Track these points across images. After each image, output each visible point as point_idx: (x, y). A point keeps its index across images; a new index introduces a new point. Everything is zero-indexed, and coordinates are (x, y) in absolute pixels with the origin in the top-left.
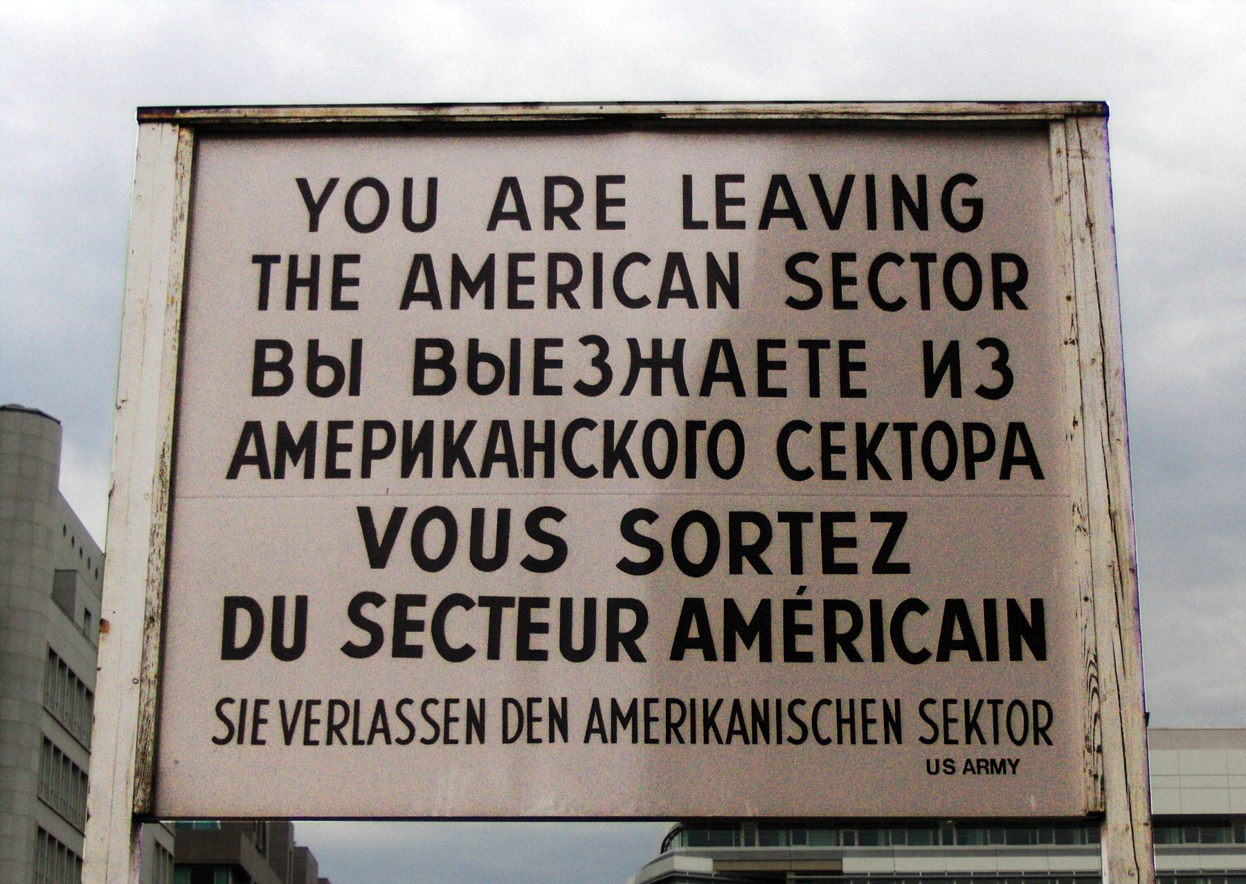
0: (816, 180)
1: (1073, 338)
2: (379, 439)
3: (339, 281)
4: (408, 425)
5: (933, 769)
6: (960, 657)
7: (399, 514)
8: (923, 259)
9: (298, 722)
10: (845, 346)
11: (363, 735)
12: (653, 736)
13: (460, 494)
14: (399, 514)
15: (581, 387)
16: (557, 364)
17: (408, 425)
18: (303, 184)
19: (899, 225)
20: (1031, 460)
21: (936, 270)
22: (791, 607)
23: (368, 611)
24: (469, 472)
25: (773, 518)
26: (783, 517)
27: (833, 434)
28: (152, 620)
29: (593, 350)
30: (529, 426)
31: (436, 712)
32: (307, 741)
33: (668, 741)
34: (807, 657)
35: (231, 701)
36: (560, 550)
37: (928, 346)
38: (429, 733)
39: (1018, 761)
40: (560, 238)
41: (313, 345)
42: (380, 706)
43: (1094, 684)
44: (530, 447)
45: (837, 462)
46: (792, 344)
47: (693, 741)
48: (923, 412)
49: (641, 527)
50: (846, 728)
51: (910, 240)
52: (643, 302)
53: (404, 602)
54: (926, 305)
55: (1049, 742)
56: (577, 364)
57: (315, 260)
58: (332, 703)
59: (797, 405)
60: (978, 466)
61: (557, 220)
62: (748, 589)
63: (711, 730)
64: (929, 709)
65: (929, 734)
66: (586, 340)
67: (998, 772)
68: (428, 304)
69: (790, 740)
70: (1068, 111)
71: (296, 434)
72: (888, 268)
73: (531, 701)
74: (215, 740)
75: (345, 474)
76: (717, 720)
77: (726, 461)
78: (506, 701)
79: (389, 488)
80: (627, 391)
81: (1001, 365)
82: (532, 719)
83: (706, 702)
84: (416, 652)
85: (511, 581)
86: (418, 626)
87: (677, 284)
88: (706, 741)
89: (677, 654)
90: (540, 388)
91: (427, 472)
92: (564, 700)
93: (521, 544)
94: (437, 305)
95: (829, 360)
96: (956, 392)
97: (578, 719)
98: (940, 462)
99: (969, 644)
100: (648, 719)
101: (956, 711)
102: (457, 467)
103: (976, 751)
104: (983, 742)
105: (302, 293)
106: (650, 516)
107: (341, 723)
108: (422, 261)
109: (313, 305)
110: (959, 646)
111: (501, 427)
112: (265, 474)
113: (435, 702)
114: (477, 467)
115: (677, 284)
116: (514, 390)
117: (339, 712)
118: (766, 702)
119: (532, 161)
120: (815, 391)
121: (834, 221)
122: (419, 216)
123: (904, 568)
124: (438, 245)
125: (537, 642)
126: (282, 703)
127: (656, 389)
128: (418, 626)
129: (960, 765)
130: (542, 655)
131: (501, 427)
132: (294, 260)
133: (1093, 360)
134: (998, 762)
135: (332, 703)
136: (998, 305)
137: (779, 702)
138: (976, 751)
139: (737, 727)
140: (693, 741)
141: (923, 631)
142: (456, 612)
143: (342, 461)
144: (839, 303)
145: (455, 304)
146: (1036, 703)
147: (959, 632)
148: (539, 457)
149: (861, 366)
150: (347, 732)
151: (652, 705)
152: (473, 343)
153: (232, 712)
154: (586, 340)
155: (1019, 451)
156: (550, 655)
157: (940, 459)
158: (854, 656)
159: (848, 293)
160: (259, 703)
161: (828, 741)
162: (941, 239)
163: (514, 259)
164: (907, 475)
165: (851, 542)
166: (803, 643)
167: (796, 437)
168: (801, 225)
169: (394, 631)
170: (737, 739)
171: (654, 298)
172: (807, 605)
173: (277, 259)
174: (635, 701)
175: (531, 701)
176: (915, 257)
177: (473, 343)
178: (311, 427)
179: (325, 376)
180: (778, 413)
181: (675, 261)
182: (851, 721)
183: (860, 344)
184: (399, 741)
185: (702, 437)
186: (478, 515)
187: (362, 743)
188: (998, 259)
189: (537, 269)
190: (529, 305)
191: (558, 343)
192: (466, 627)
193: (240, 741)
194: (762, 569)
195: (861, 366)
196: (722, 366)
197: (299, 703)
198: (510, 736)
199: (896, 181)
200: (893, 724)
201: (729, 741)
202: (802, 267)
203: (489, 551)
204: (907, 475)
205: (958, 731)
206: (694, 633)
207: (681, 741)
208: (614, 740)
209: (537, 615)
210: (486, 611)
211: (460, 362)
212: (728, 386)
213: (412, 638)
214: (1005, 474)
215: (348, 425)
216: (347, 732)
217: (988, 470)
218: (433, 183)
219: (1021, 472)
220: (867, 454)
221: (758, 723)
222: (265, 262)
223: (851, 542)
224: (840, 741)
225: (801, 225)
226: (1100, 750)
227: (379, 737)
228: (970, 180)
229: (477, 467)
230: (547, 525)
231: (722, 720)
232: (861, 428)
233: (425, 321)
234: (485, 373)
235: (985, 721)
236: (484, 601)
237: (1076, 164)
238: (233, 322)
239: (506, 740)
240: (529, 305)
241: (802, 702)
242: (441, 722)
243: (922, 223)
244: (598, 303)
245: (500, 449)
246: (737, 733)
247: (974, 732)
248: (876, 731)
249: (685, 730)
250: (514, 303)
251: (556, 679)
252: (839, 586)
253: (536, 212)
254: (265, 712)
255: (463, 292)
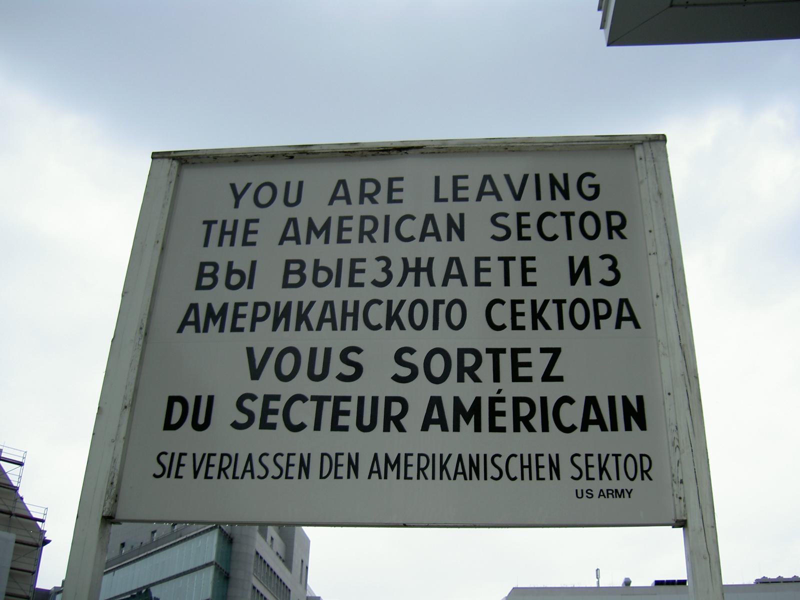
0: (508, 177)
1: (654, 251)
2: (262, 311)
3: (247, 232)
4: (278, 304)
5: (580, 495)
6: (594, 429)
7: (269, 351)
8: (568, 215)
9: (203, 466)
10: (524, 260)
11: (239, 473)
12: (408, 476)
13: (303, 340)
14: (269, 351)
15: (375, 283)
16: (363, 271)
17: (278, 304)
18: (233, 186)
19: (553, 197)
20: (633, 318)
21: (575, 221)
22: (493, 401)
23: (247, 404)
24: (310, 328)
25: (483, 352)
26: (488, 351)
27: (517, 305)
28: (126, 407)
29: (383, 264)
30: (345, 304)
31: (282, 461)
32: (206, 477)
33: (418, 478)
34: (503, 430)
35: (166, 453)
36: (359, 369)
37: (571, 259)
38: (277, 475)
39: (631, 490)
40: (368, 208)
41: (230, 264)
42: (250, 456)
43: (676, 443)
44: (345, 314)
45: (520, 321)
46: (494, 259)
47: (433, 478)
48: (570, 293)
49: (406, 357)
50: (526, 470)
51: (560, 205)
52: (412, 239)
53: (268, 398)
54: (569, 237)
55: (650, 479)
56: (374, 271)
57: (236, 222)
58: (223, 455)
59: (497, 290)
60: (602, 322)
61: (366, 200)
62: (468, 392)
63: (444, 472)
64: (576, 459)
65: (577, 474)
66: (379, 259)
67: (620, 496)
68: (294, 242)
69: (492, 478)
70: (644, 139)
71: (217, 310)
72: (548, 219)
73: (337, 455)
74: (155, 476)
75: (241, 330)
76: (448, 466)
77: (456, 321)
78: (323, 455)
79: (265, 337)
80: (400, 284)
81: (613, 268)
82: (337, 465)
83: (441, 455)
84: (273, 426)
85: (331, 387)
86: (275, 412)
87: (430, 229)
88: (441, 478)
89: (425, 428)
90: (352, 284)
91: (287, 328)
92: (357, 454)
93: (337, 366)
94: (298, 243)
95: (515, 268)
96: (588, 282)
97: (364, 466)
98: (580, 320)
99: (600, 422)
100: (406, 465)
101: (593, 461)
102: (303, 326)
103: (606, 484)
104: (610, 479)
105: (227, 238)
106: (411, 351)
107: (225, 466)
108: (293, 221)
109: (232, 244)
110: (594, 422)
111: (328, 304)
112: (198, 330)
113: (282, 455)
114: (314, 324)
115: (430, 229)
116: (338, 285)
117: (226, 459)
118: (478, 456)
119: (353, 173)
120: (507, 283)
121: (518, 197)
122: (292, 198)
123: (560, 379)
124: (301, 214)
125: (342, 421)
126: (194, 455)
127: (417, 283)
128: (275, 412)
129: (596, 493)
130: (345, 429)
131: (328, 304)
132: (224, 222)
133: (666, 263)
134: (620, 492)
135: (223, 455)
136: (610, 237)
137: (485, 456)
138: (606, 484)
139: (460, 470)
140: (433, 478)
141: (572, 415)
142: (298, 404)
143: (240, 323)
144: (520, 237)
145: (308, 242)
146: (641, 456)
147: (593, 415)
148: (350, 320)
149: (534, 270)
150: (230, 472)
151: (409, 457)
152: (317, 262)
153: (166, 460)
154: (379, 259)
155: (626, 313)
156: (350, 429)
157: (580, 319)
158: (531, 429)
159: (525, 232)
160: (181, 455)
161: (515, 478)
162: (577, 205)
163: (342, 219)
164: (561, 327)
165: (529, 365)
166: (499, 421)
167: (497, 306)
168: (499, 198)
169: (262, 415)
170: (460, 477)
171: (418, 237)
172: (502, 400)
173: (215, 222)
174: (399, 455)
175: (337, 455)
176: (562, 214)
177: (317, 262)
178: (225, 306)
179: (235, 279)
180: (488, 294)
181: (430, 218)
182: (529, 467)
183: (533, 259)
184: (259, 477)
185: (442, 309)
186: (313, 351)
187: (238, 478)
188: (609, 214)
189: (354, 224)
190: (349, 241)
191: (364, 260)
192: (303, 413)
193: (169, 476)
194: (476, 379)
195: (534, 270)
196: (454, 271)
197: (204, 455)
198: (324, 475)
199: (551, 176)
200: (555, 468)
201: (455, 479)
202: (500, 220)
203: (318, 371)
204: (561, 327)
205: (594, 472)
206: (435, 415)
207: (426, 478)
208: (386, 478)
209: (344, 406)
210: (315, 403)
211: (309, 271)
212: (458, 281)
213: (271, 419)
214: (618, 326)
215: (245, 304)
216: (230, 472)
217: (608, 324)
218: (301, 184)
219: (627, 325)
220: (537, 316)
221: (473, 468)
222: (209, 224)
223: (529, 365)
224: (523, 479)
225: (499, 198)
226: (682, 482)
227: (248, 475)
228: (593, 175)
229: (314, 324)
230: (352, 356)
231: (451, 466)
232: (534, 303)
233: (291, 250)
234: (322, 276)
235: (611, 466)
236: (313, 398)
237: (650, 165)
238: (191, 253)
239: (321, 477)
240: (349, 241)
241: (500, 456)
242: (284, 466)
243: (566, 196)
244: (386, 240)
245: (328, 315)
246: (460, 473)
247: (604, 472)
248: (545, 472)
249: (429, 472)
250: (340, 240)
251: (352, 442)
252: (521, 389)
253: (355, 195)
254: (184, 460)
255: (313, 235)
